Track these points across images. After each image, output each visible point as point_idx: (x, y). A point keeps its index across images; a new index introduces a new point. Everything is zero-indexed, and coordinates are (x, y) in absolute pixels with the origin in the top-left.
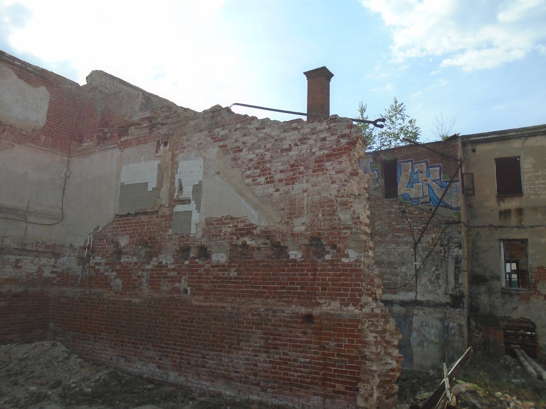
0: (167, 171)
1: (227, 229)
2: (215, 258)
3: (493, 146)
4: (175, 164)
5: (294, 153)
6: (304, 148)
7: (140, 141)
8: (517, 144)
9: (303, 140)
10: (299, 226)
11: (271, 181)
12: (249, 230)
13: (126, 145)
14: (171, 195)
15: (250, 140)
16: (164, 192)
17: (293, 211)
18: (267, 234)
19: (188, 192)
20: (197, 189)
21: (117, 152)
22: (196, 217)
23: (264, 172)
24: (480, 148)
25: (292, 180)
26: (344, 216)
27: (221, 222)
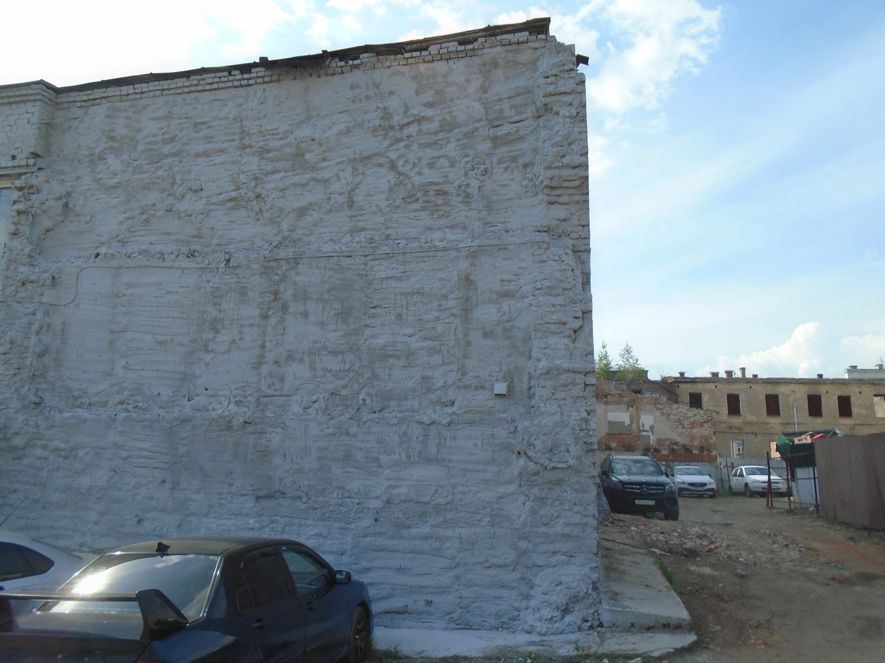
0: (635, 418)
1: (668, 442)
2: (663, 453)
3: (688, 385)
4: (639, 417)
5: (692, 419)
6: (696, 418)
7: (616, 403)
8: (700, 386)
9: (695, 415)
10: (696, 443)
11: (683, 427)
12: (676, 444)
13: (607, 403)
14: (638, 428)
15: (674, 412)
16: (634, 426)
17: (693, 438)
18: (684, 446)
19: (647, 427)
20: (652, 427)
21: (603, 406)
22: (652, 437)
23: (681, 424)
24: (681, 385)
25: (692, 428)
26: (711, 441)
27: (664, 440)
